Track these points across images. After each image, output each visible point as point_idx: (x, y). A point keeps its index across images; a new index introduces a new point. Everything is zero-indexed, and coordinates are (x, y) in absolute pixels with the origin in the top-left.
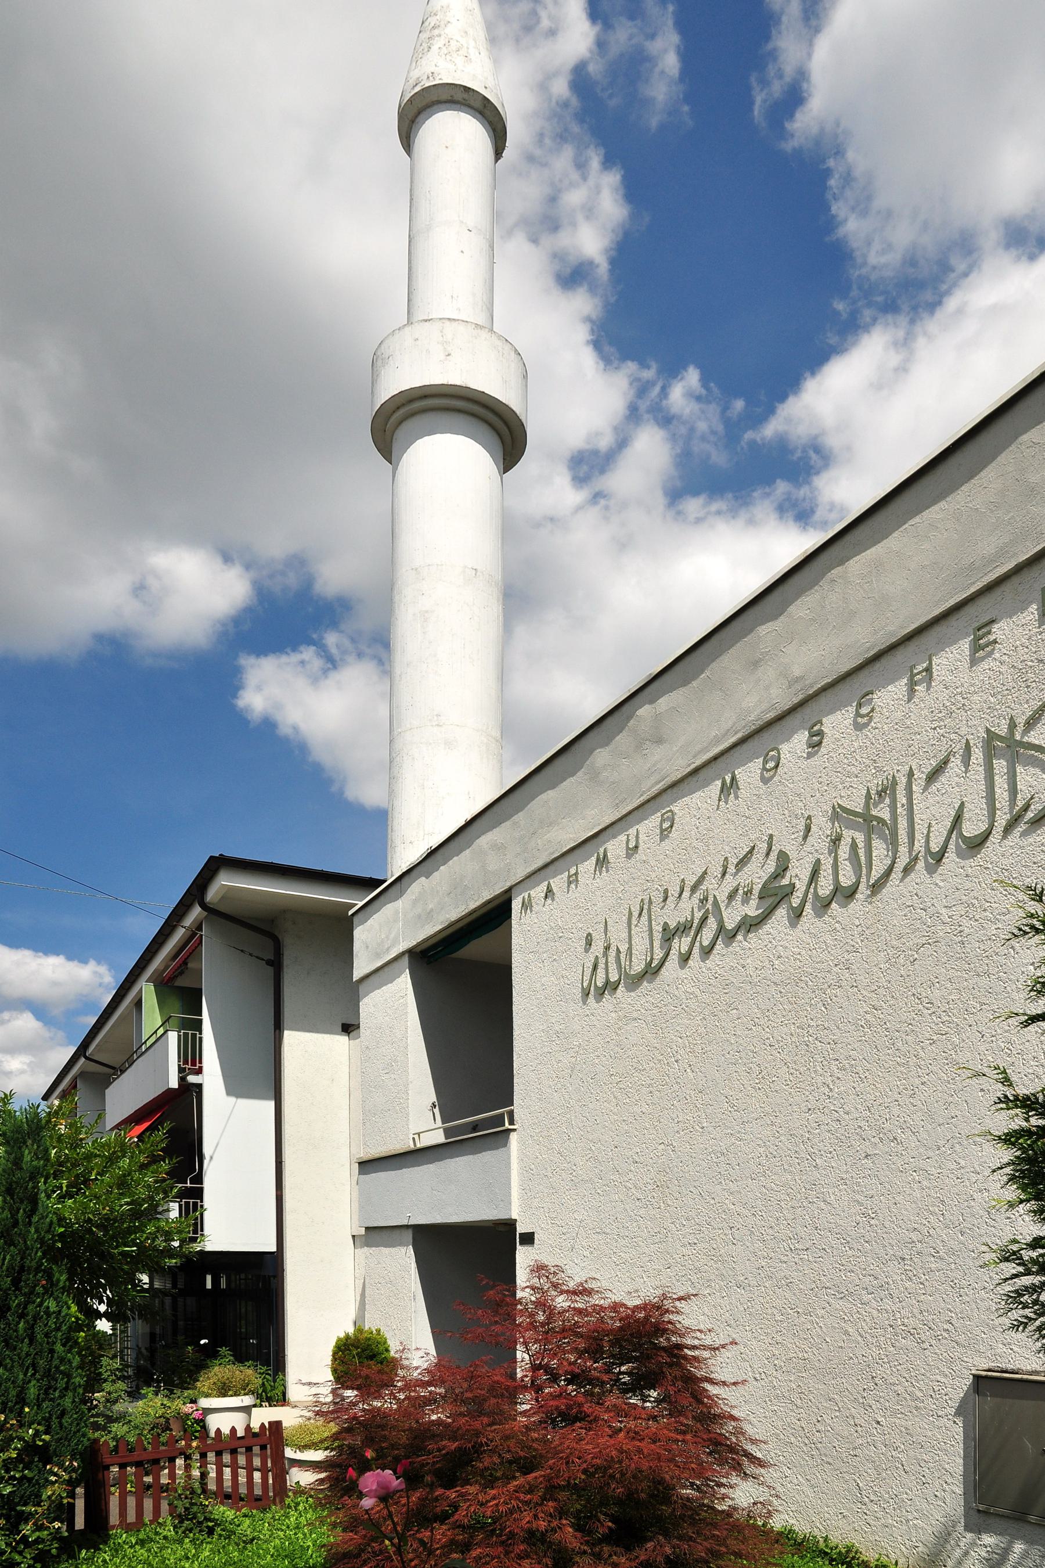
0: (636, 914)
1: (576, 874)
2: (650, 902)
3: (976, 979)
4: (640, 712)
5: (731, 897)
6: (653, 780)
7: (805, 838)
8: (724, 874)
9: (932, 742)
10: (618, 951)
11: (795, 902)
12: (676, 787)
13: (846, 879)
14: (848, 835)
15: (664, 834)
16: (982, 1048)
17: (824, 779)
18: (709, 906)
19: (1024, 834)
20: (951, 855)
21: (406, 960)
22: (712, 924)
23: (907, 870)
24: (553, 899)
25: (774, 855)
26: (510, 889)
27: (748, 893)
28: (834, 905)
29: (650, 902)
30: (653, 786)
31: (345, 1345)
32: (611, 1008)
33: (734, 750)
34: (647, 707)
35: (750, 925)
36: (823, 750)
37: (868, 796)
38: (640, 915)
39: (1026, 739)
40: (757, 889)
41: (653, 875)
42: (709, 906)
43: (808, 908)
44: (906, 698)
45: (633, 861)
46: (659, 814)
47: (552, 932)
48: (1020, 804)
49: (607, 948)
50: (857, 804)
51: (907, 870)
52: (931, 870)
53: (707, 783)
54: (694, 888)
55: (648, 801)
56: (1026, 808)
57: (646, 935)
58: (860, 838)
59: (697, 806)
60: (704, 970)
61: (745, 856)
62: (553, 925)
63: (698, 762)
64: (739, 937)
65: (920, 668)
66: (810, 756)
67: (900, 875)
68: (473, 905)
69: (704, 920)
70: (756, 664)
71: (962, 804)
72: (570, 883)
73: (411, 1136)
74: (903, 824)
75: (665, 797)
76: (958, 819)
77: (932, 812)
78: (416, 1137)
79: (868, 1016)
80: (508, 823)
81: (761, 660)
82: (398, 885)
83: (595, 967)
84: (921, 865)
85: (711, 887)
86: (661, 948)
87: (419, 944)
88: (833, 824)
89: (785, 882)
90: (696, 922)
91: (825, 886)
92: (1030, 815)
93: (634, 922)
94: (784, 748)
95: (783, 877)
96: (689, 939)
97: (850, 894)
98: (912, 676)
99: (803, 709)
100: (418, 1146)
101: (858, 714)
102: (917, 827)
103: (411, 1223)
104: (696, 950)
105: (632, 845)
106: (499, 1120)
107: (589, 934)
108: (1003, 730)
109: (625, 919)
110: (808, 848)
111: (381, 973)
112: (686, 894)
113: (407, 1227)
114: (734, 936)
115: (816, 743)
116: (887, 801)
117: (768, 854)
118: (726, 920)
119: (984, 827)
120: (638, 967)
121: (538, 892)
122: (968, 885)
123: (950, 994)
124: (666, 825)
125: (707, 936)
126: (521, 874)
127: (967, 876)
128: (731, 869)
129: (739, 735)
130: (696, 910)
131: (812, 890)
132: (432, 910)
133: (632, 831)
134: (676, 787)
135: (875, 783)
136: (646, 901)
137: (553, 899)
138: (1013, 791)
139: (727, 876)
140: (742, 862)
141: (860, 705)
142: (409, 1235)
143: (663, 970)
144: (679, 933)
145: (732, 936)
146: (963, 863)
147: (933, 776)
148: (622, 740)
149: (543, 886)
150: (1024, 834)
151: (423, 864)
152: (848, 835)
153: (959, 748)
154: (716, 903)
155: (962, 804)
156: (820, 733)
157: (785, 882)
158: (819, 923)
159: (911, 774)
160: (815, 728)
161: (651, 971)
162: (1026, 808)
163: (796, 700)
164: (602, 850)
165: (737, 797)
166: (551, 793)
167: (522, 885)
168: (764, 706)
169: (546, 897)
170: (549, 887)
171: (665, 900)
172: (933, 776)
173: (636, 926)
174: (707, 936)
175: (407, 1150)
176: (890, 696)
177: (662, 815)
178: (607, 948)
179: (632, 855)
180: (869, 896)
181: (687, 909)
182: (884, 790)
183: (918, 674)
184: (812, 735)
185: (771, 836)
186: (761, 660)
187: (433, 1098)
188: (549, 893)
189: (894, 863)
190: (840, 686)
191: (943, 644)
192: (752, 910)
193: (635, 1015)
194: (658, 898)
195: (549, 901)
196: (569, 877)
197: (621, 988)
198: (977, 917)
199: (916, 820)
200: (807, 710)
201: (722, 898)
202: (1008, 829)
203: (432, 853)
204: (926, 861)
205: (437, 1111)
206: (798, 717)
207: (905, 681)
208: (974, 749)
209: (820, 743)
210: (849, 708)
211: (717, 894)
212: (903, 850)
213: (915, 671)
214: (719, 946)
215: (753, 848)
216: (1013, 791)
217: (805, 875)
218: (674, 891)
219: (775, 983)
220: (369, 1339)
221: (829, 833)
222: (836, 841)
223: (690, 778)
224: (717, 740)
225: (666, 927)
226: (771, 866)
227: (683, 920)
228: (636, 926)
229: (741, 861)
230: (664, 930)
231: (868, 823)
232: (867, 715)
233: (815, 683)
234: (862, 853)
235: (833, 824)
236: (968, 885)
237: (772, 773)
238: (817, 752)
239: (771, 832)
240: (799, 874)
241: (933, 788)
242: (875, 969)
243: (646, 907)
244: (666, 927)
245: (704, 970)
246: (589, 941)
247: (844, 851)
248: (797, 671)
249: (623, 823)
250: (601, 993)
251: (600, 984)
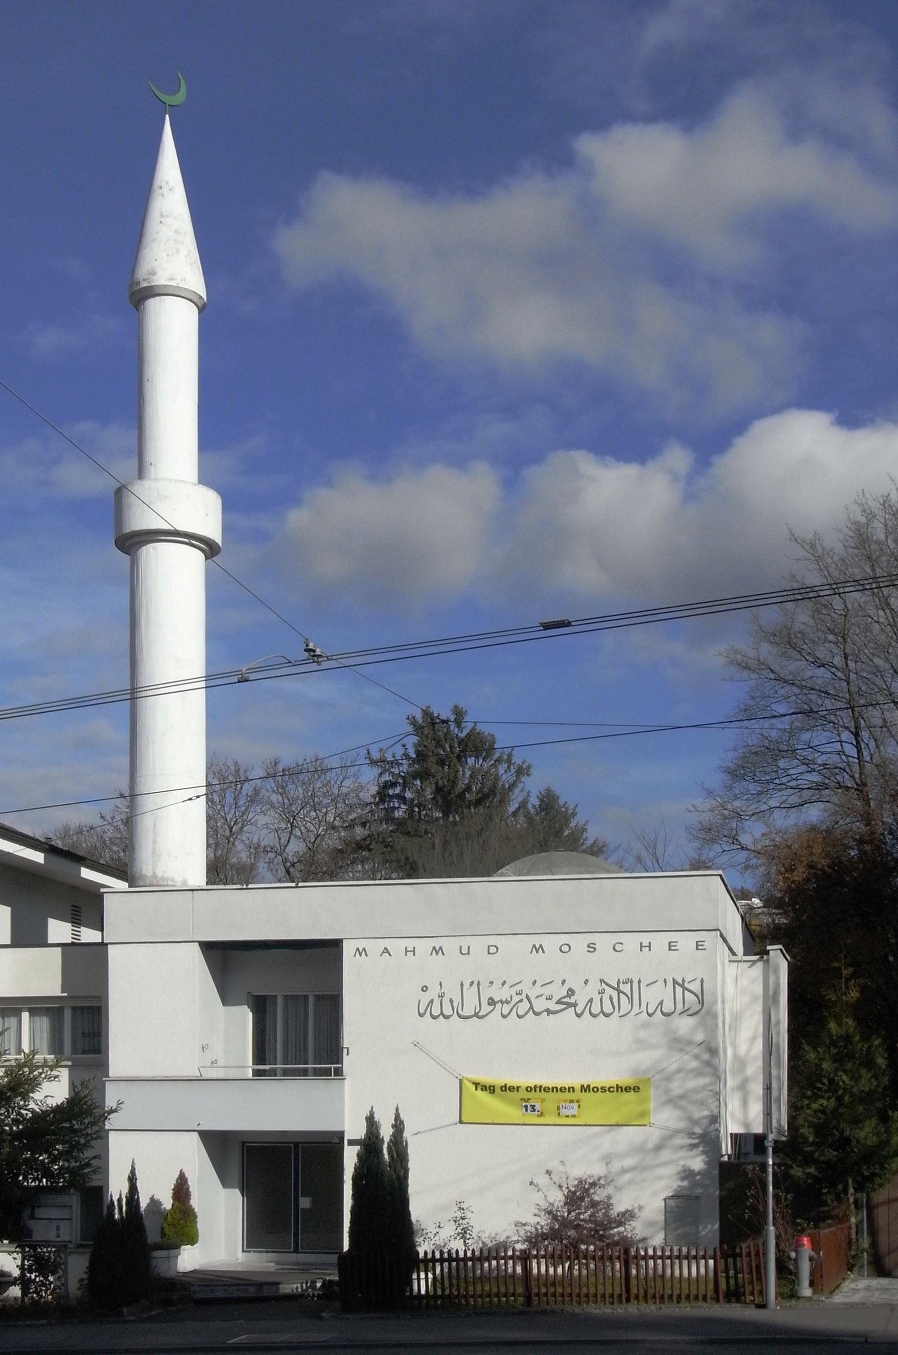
13: (608, 1008)
35: (549, 1012)
40: (555, 999)
48: (686, 1008)
90: (513, 1003)
128: (538, 984)
157: (572, 1000)
222: (601, 992)
225: (491, 999)
240: (581, 998)
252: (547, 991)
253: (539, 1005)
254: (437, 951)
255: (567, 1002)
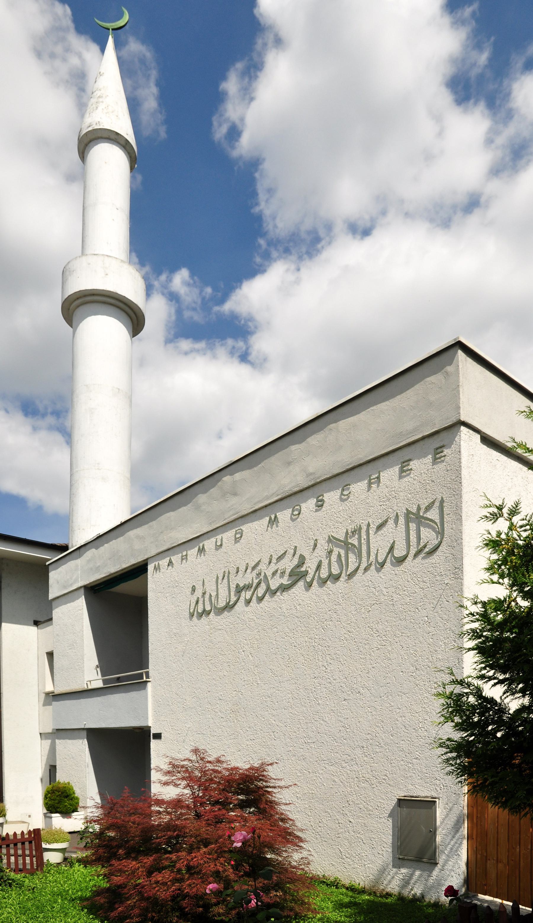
0: (220, 578)
1: (186, 555)
2: (229, 573)
3: (400, 621)
4: (225, 479)
5: (274, 574)
6: (231, 513)
7: (314, 549)
8: (270, 563)
9: (379, 512)
10: (211, 595)
11: (308, 579)
12: (244, 518)
13: (335, 570)
14: (336, 550)
15: (237, 540)
16: (402, 653)
17: (324, 522)
18: (262, 577)
19: (423, 558)
20: (388, 565)
21: (82, 590)
22: (263, 587)
23: (366, 569)
24: (172, 567)
25: (297, 556)
26: (147, 559)
27: (283, 573)
28: (328, 582)
29: (229, 573)
30: (231, 516)
31: (51, 790)
32: (206, 623)
33: (277, 503)
34: (228, 477)
35: (284, 588)
36: (323, 509)
37: (347, 533)
38: (223, 579)
39: (425, 516)
40: (288, 572)
41: (231, 560)
42: (262, 577)
43: (315, 583)
44: (367, 490)
45: (219, 551)
46: (234, 530)
47: (172, 583)
48: (422, 544)
49: (204, 594)
50: (341, 536)
51: (366, 569)
52: (378, 570)
53: (261, 518)
54: (254, 568)
55: (228, 523)
56: (425, 546)
57: (226, 589)
58: (342, 552)
59: (255, 529)
60: (259, 608)
61: (283, 554)
62: (172, 580)
63: (257, 507)
64: (278, 594)
65: (374, 477)
66: (317, 511)
67: (363, 571)
68: (124, 566)
69: (259, 584)
70: (289, 463)
71: (394, 541)
72: (182, 559)
73: (86, 682)
74: (364, 548)
75: (237, 522)
76: (392, 548)
77: (379, 544)
78: (89, 683)
79: (346, 635)
80: (146, 526)
81: (291, 462)
82: (78, 551)
83: (197, 602)
84: (373, 567)
85: (263, 568)
86: (235, 595)
87: (90, 583)
88: (329, 544)
89: (303, 569)
90: (254, 585)
91: (324, 573)
92: (427, 550)
93: (220, 582)
94: (303, 506)
95: (302, 567)
96: (251, 593)
97: (337, 578)
98: (370, 480)
99: (315, 488)
100: (90, 687)
101: (342, 494)
102: (371, 550)
103: (87, 727)
104: (254, 598)
105: (219, 544)
106: (140, 676)
107: (194, 586)
108: (414, 510)
109: (214, 580)
110: (315, 554)
111: (68, 597)
112: (249, 570)
113: (83, 729)
114: (276, 593)
115: (320, 505)
116: (357, 536)
117: (294, 555)
118: (271, 585)
119: (404, 553)
120: (222, 604)
121: (164, 562)
122: (396, 579)
123: (387, 628)
124: (238, 536)
125: (261, 591)
126: (153, 552)
127: (396, 574)
128: (274, 560)
129: (279, 497)
130: (254, 579)
131: (317, 574)
132: (99, 566)
133: (219, 537)
134: (244, 518)
135: (350, 528)
136: (227, 572)
137: (172, 567)
138: (419, 538)
139: (272, 564)
140: (280, 558)
141: (343, 490)
142: (85, 733)
143: (236, 607)
144: (245, 589)
145: (274, 593)
146: (394, 568)
147: (380, 527)
148: (214, 491)
149: (167, 560)
150: (423, 558)
151: (94, 542)
152: (336, 550)
153: (393, 516)
154: (265, 576)
155: (394, 541)
156: (322, 500)
157: (303, 569)
158: (320, 590)
159: (369, 525)
160: (320, 498)
161: (229, 607)
162: (425, 546)
163: (310, 484)
164: (201, 545)
165: (277, 526)
166: (172, 514)
167: (154, 558)
168: (293, 484)
169: (169, 565)
170: (170, 559)
171: (237, 572)
172: (380, 527)
173: (221, 584)
174: (261, 591)
175: (84, 689)
176: (358, 488)
177: (236, 531)
178: (204, 594)
179: (219, 549)
180: (346, 580)
181: (249, 578)
182: (355, 531)
183: (373, 479)
184: (318, 501)
185: (296, 547)
186: (291, 462)
187: (97, 663)
188: (170, 563)
189: (359, 565)
190: (333, 480)
191: (386, 467)
192: (285, 581)
193: (220, 627)
194: (233, 571)
195: (170, 567)
196: (182, 556)
197: (212, 614)
198: (400, 594)
199: (371, 546)
200: (316, 489)
201: (269, 574)
202: (416, 555)
203: (99, 537)
204: (376, 566)
205: (99, 669)
206: (310, 492)
207: (366, 481)
208: (400, 517)
209: (322, 505)
210: (337, 491)
211: (266, 572)
212: (364, 559)
213: (372, 478)
214: (267, 597)
215: (286, 552)
216: (419, 538)
217: (314, 567)
218: (242, 568)
219: (297, 617)
220: (65, 787)
221: (326, 548)
222: (330, 552)
223: (251, 514)
224: (267, 498)
225: (237, 586)
226: (296, 561)
227: (247, 583)
228: (221, 584)
229: (280, 557)
230: (237, 587)
231: (346, 545)
232: (347, 495)
233: (320, 477)
234: (343, 559)
235: (329, 544)
236: (396, 579)
237: (296, 517)
238: (320, 510)
239: (295, 545)
240: (310, 566)
241: (380, 533)
242: (349, 614)
243: (226, 575)
244: (237, 586)
245: (259, 608)
246: (194, 589)
247: (334, 558)
248: (311, 470)
249: (214, 532)
250: (200, 616)
251: (200, 611)
252: (281, 565)
253: (274, 584)
254: (202, 551)
255: (297, 575)
